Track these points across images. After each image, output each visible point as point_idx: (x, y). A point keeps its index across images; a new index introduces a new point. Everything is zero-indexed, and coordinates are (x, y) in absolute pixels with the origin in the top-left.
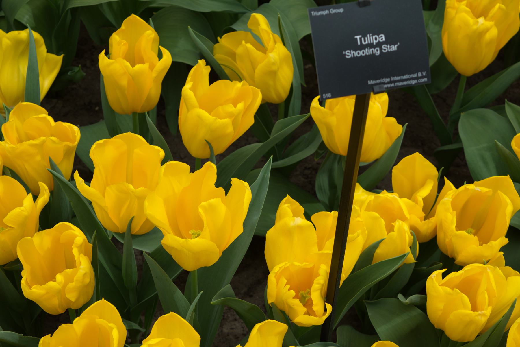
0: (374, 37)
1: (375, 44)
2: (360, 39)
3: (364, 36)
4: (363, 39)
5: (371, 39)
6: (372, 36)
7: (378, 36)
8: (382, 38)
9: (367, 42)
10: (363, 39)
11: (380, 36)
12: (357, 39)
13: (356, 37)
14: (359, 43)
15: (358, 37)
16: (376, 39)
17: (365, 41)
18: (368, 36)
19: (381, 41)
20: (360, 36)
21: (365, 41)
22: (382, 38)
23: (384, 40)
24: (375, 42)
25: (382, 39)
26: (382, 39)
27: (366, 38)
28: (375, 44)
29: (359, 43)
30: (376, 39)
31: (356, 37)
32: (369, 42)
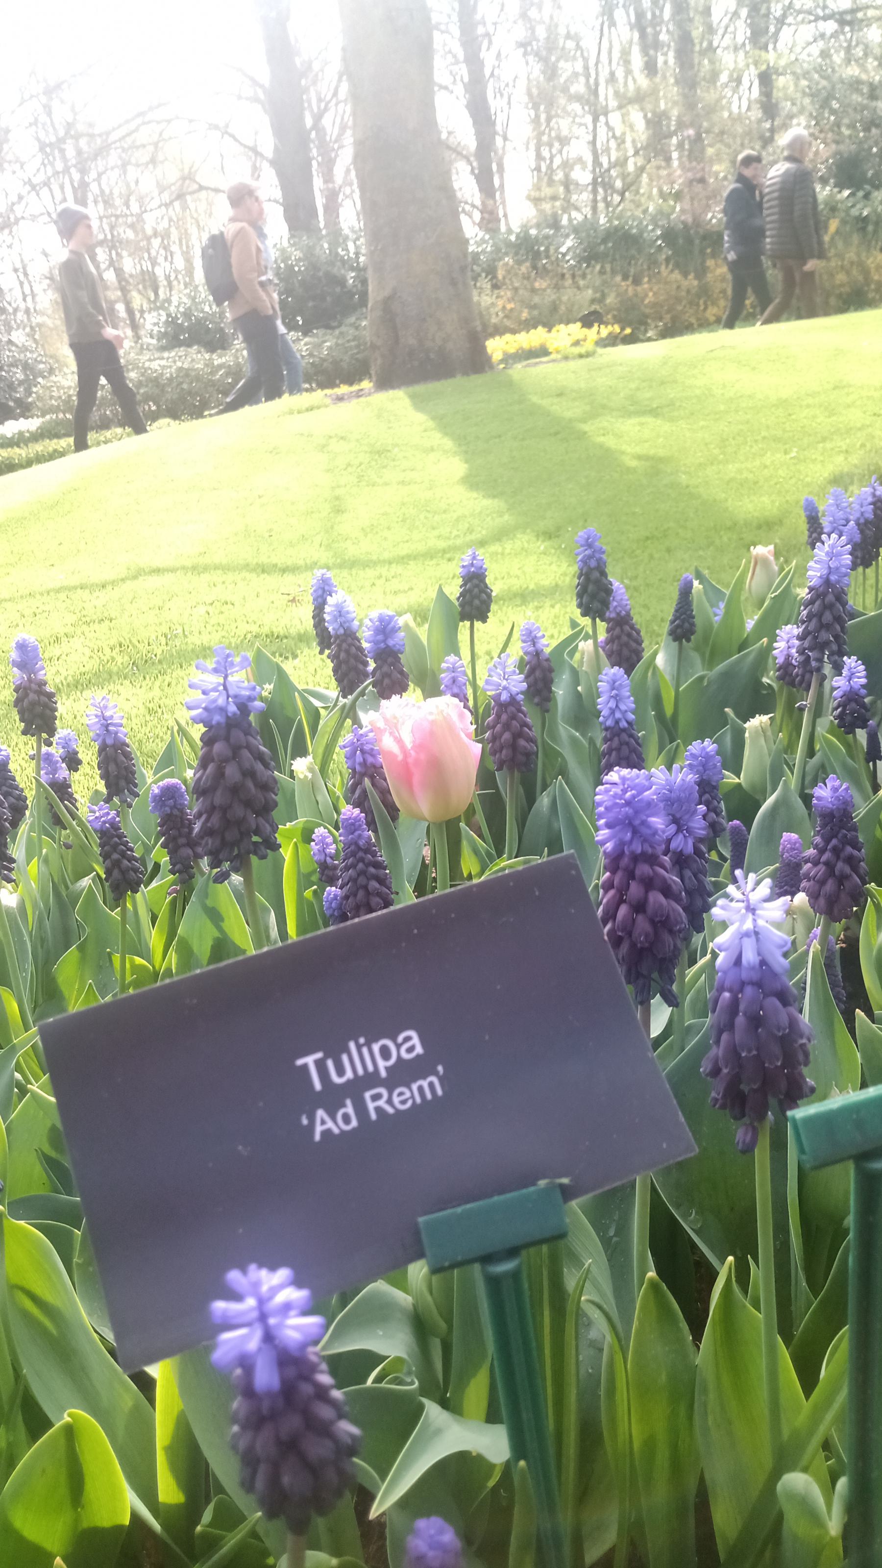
0: (376, 1047)
1: (383, 1074)
3: (335, 1050)
4: (330, 1064)
6: (368, 1044)
7: (394, 1040)
8: (411, 1044)
9: (349, 1074)
10: (330, 1064)
11: (400, 1039)
12: (305, 1067)
13: (300, 1062)
14: (318, 1086)
15: (310, 1060)
16: (385, 1053)
17: (341, 1072)
18: (352, 1045)
19: (405, 1056)
20: (319, 1055)
21: (341, 1072)
22: (411, 1044)
23: (419, 1050)
24: (382, 1064)
25: (410, 1050)
26: (410, 1050)
27: (345, 1058)
28: (383, 1074)
29: (318, 1086)
30: (385, 1053)
31: (300, 1062)
32: (360, 1072)
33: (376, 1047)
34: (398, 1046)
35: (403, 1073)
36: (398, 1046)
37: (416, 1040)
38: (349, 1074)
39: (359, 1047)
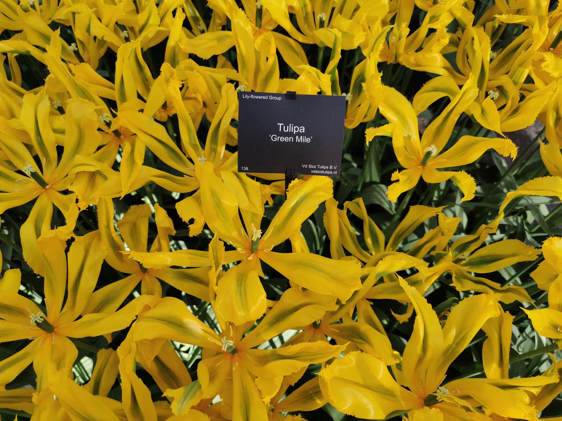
0: (295, 127)
2: (282, 126)
3: (286, 125)
8: (303, 129)
9: (287, 131)
15: (280, 124)
17: (286, 129)
21: (286, 129)
22: (303, 129)
23: (304, 131)
24: (295, 131)
33: (295, 127)
35: (299, 134)
37: (304, 129)
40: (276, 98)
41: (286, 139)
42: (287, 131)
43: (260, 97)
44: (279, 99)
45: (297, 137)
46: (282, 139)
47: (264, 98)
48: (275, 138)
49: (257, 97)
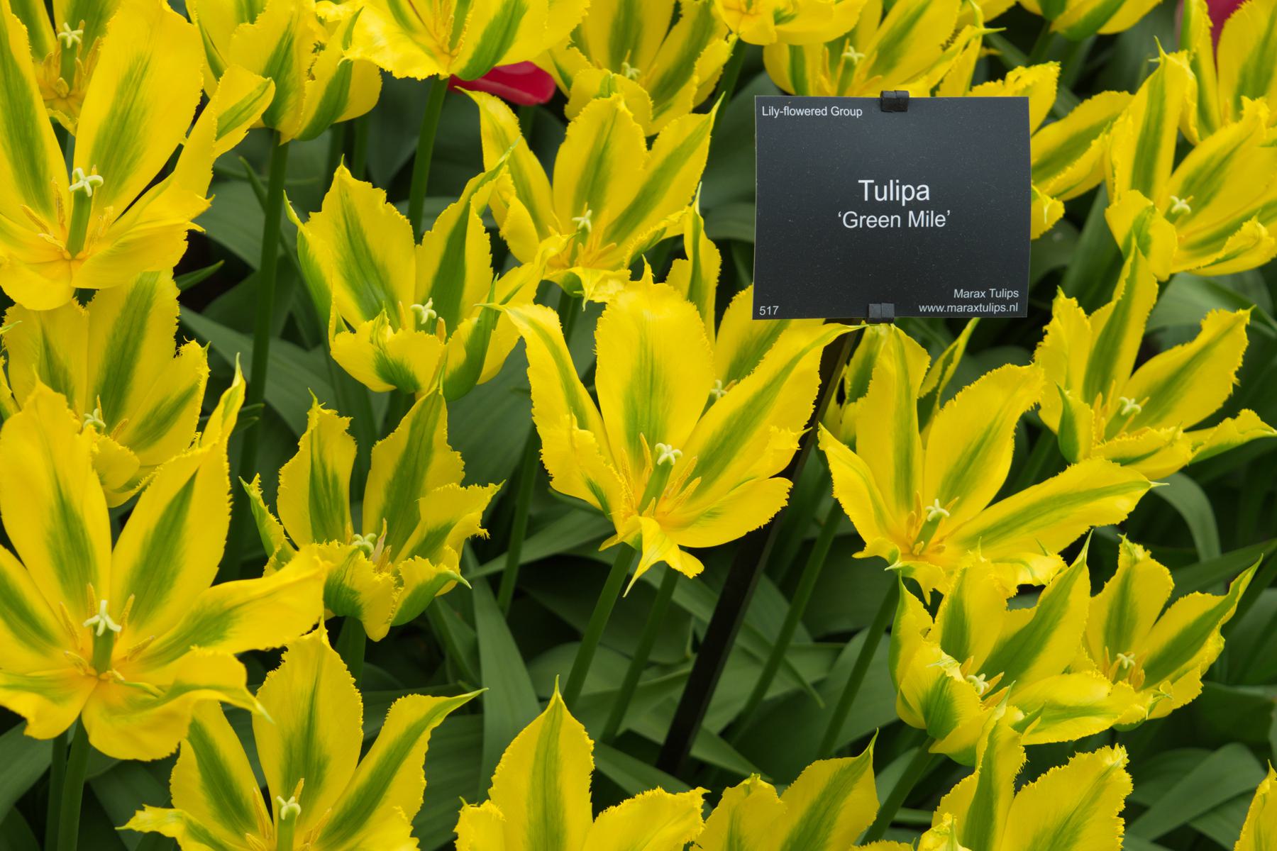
2: (871, 187)
3: (882, 182)
5: (895, 191)
15: (866, 182)
16: (908, 193)
17: (881, 195)
21: (881, 195)
22: (924, 193)
23: (927, 197)
24: (904, 198)
26: (922, 196)
30: (908, 193)
33: (904, 188)
34: (917, 192)
35: (916, 206)
36: (917, 192)
37: (927, 192)
38: (885, 198)
39: (895, 185)
40: (850, 112)
41: (883, 221)
42: (885, 198)
43: (807, 112)
44: (858, 113)
45: (911, 213)
46: (873, 221)
47: (818, 112)
48: (852, 221)
49: (800, 112)
